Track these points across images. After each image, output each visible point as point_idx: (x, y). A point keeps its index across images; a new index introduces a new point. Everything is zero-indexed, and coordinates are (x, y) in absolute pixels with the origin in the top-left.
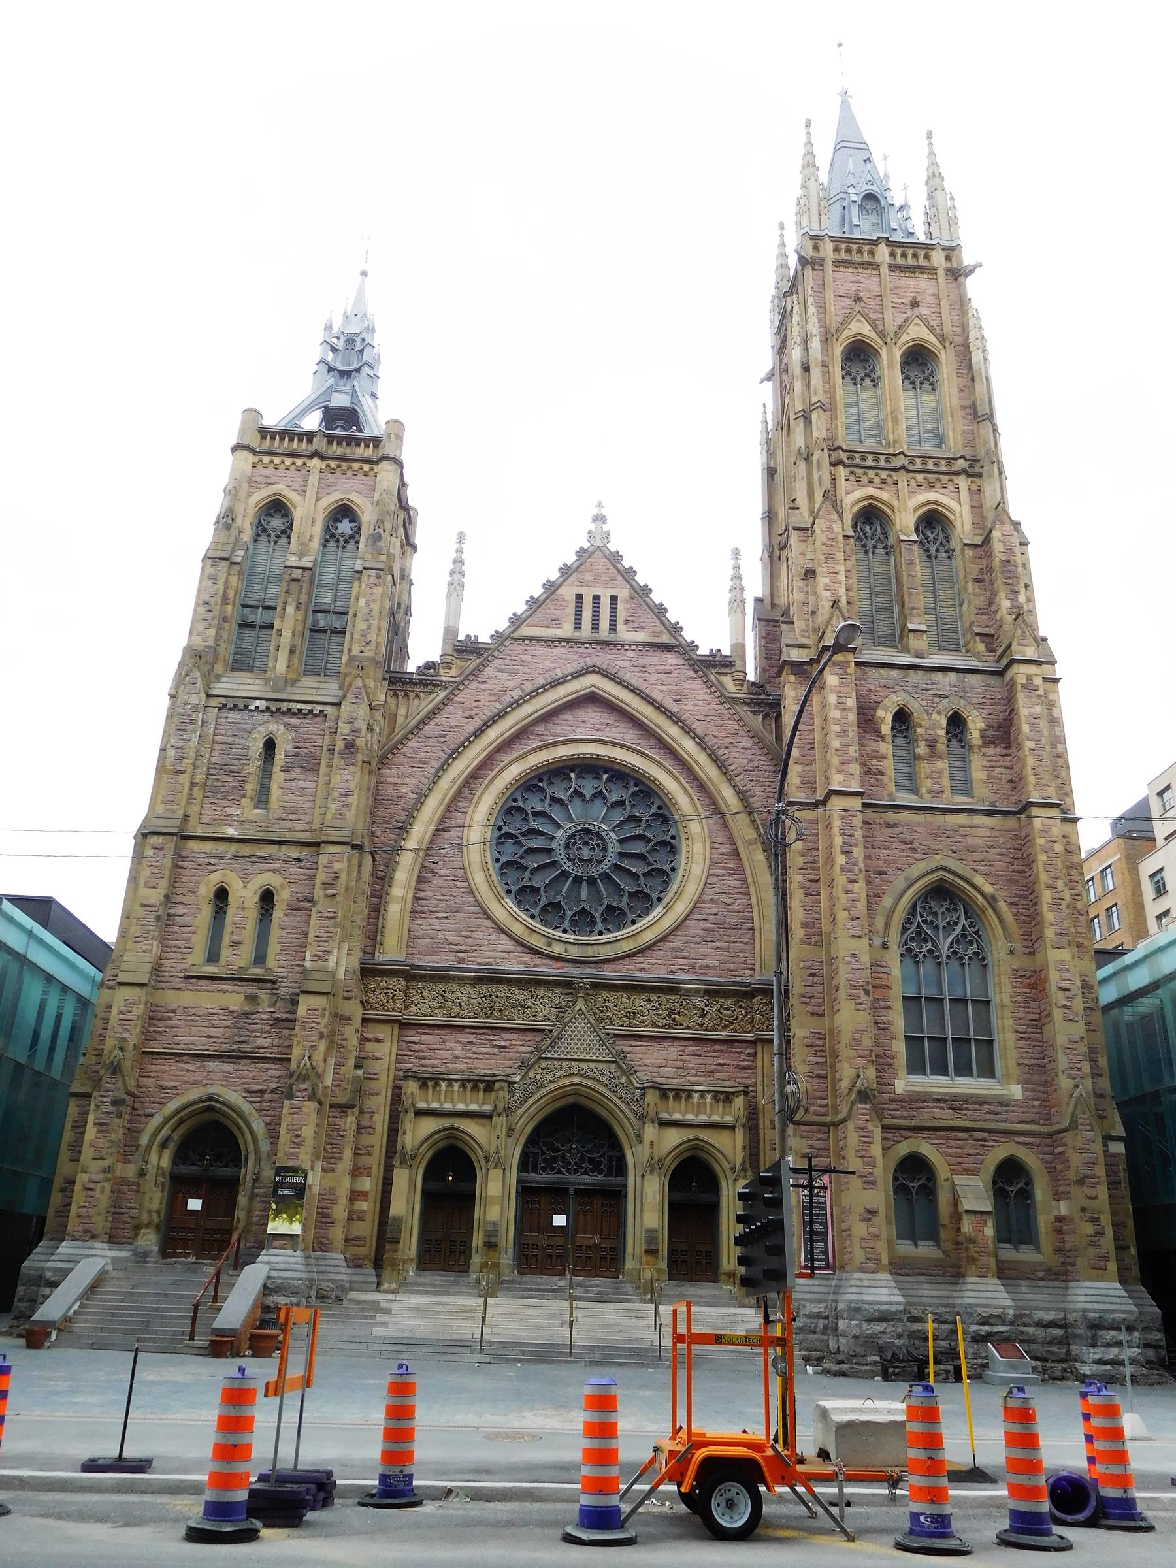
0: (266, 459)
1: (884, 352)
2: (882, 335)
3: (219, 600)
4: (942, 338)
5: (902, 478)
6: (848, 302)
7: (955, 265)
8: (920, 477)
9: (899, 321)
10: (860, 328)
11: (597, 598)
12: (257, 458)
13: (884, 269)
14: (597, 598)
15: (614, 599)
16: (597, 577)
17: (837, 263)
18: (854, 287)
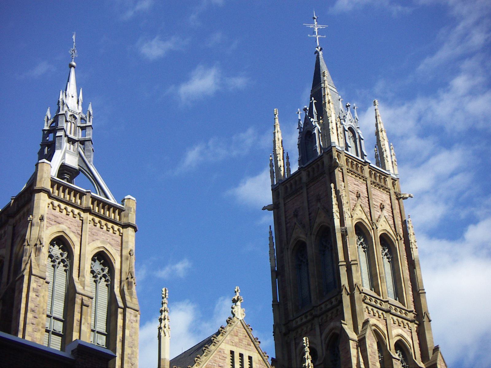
0: (56, 203)
1: (372, 233)
2: (372, 224)
3: (41, 310)
4: (397, 234)
5: (389, 317)
6: (354, 197)
7: (397, 191)
8: (395, 318)
9: (377, 217)
10: (360, 215)
11: (241, 355)
12: (50, 201)
13: (369, 182)
14: (241, 355)
15: (250, 358)
16: (241, 340)
17: (350, 171)
18: (356, 189)
